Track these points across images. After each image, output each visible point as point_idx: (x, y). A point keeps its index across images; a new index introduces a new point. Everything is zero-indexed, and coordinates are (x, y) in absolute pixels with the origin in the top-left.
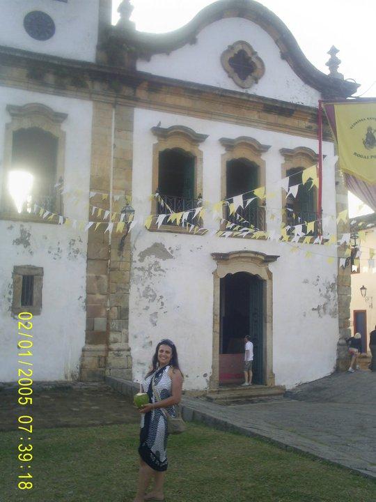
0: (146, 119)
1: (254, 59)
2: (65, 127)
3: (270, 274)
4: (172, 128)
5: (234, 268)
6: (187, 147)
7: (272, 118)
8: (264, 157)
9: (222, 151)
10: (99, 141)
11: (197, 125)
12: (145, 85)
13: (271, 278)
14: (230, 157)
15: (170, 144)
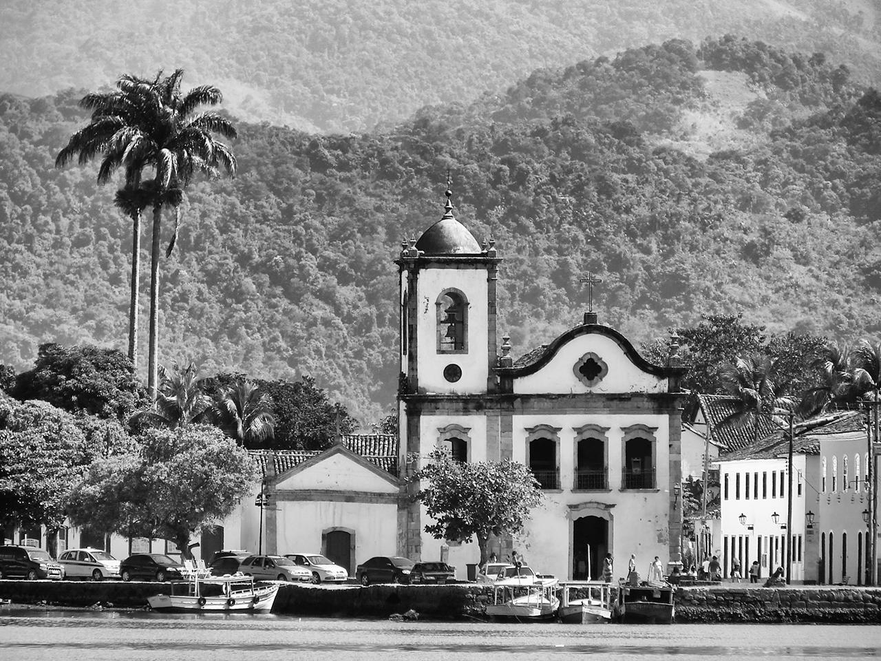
0: (521, 422)
1: (599, 364)
2: (470, 434)
3: (611, 516)
4: (537, 426)
5: (584, 514)
6: (549, 436)
7: (615, 403)
8: (607, 434)
9: (575, 434)
10: (491, 439)
11: (553, 420)
12: (519, 399)
13: (612, 519)
14: (579, 439)
15: (536, 436)
